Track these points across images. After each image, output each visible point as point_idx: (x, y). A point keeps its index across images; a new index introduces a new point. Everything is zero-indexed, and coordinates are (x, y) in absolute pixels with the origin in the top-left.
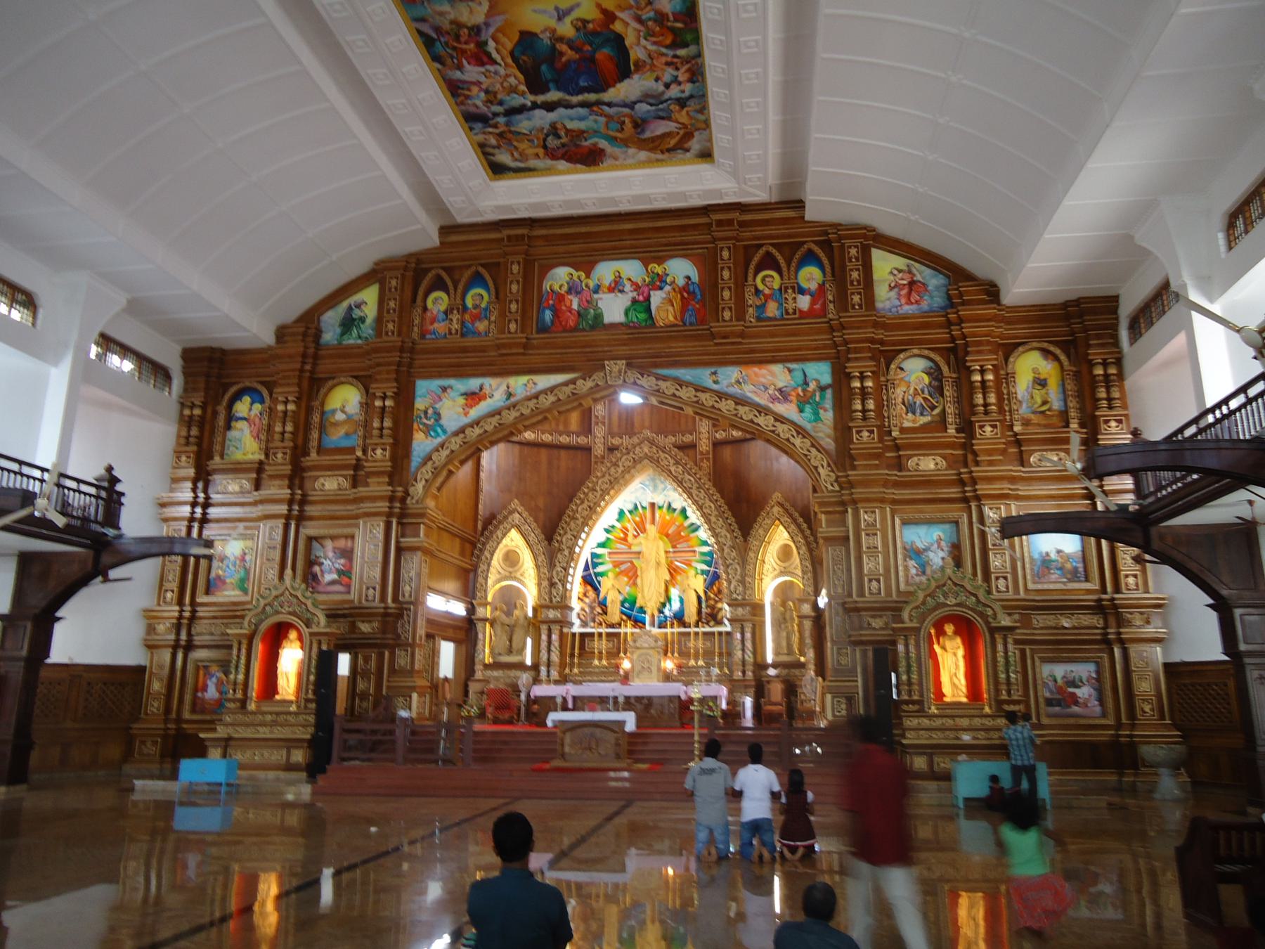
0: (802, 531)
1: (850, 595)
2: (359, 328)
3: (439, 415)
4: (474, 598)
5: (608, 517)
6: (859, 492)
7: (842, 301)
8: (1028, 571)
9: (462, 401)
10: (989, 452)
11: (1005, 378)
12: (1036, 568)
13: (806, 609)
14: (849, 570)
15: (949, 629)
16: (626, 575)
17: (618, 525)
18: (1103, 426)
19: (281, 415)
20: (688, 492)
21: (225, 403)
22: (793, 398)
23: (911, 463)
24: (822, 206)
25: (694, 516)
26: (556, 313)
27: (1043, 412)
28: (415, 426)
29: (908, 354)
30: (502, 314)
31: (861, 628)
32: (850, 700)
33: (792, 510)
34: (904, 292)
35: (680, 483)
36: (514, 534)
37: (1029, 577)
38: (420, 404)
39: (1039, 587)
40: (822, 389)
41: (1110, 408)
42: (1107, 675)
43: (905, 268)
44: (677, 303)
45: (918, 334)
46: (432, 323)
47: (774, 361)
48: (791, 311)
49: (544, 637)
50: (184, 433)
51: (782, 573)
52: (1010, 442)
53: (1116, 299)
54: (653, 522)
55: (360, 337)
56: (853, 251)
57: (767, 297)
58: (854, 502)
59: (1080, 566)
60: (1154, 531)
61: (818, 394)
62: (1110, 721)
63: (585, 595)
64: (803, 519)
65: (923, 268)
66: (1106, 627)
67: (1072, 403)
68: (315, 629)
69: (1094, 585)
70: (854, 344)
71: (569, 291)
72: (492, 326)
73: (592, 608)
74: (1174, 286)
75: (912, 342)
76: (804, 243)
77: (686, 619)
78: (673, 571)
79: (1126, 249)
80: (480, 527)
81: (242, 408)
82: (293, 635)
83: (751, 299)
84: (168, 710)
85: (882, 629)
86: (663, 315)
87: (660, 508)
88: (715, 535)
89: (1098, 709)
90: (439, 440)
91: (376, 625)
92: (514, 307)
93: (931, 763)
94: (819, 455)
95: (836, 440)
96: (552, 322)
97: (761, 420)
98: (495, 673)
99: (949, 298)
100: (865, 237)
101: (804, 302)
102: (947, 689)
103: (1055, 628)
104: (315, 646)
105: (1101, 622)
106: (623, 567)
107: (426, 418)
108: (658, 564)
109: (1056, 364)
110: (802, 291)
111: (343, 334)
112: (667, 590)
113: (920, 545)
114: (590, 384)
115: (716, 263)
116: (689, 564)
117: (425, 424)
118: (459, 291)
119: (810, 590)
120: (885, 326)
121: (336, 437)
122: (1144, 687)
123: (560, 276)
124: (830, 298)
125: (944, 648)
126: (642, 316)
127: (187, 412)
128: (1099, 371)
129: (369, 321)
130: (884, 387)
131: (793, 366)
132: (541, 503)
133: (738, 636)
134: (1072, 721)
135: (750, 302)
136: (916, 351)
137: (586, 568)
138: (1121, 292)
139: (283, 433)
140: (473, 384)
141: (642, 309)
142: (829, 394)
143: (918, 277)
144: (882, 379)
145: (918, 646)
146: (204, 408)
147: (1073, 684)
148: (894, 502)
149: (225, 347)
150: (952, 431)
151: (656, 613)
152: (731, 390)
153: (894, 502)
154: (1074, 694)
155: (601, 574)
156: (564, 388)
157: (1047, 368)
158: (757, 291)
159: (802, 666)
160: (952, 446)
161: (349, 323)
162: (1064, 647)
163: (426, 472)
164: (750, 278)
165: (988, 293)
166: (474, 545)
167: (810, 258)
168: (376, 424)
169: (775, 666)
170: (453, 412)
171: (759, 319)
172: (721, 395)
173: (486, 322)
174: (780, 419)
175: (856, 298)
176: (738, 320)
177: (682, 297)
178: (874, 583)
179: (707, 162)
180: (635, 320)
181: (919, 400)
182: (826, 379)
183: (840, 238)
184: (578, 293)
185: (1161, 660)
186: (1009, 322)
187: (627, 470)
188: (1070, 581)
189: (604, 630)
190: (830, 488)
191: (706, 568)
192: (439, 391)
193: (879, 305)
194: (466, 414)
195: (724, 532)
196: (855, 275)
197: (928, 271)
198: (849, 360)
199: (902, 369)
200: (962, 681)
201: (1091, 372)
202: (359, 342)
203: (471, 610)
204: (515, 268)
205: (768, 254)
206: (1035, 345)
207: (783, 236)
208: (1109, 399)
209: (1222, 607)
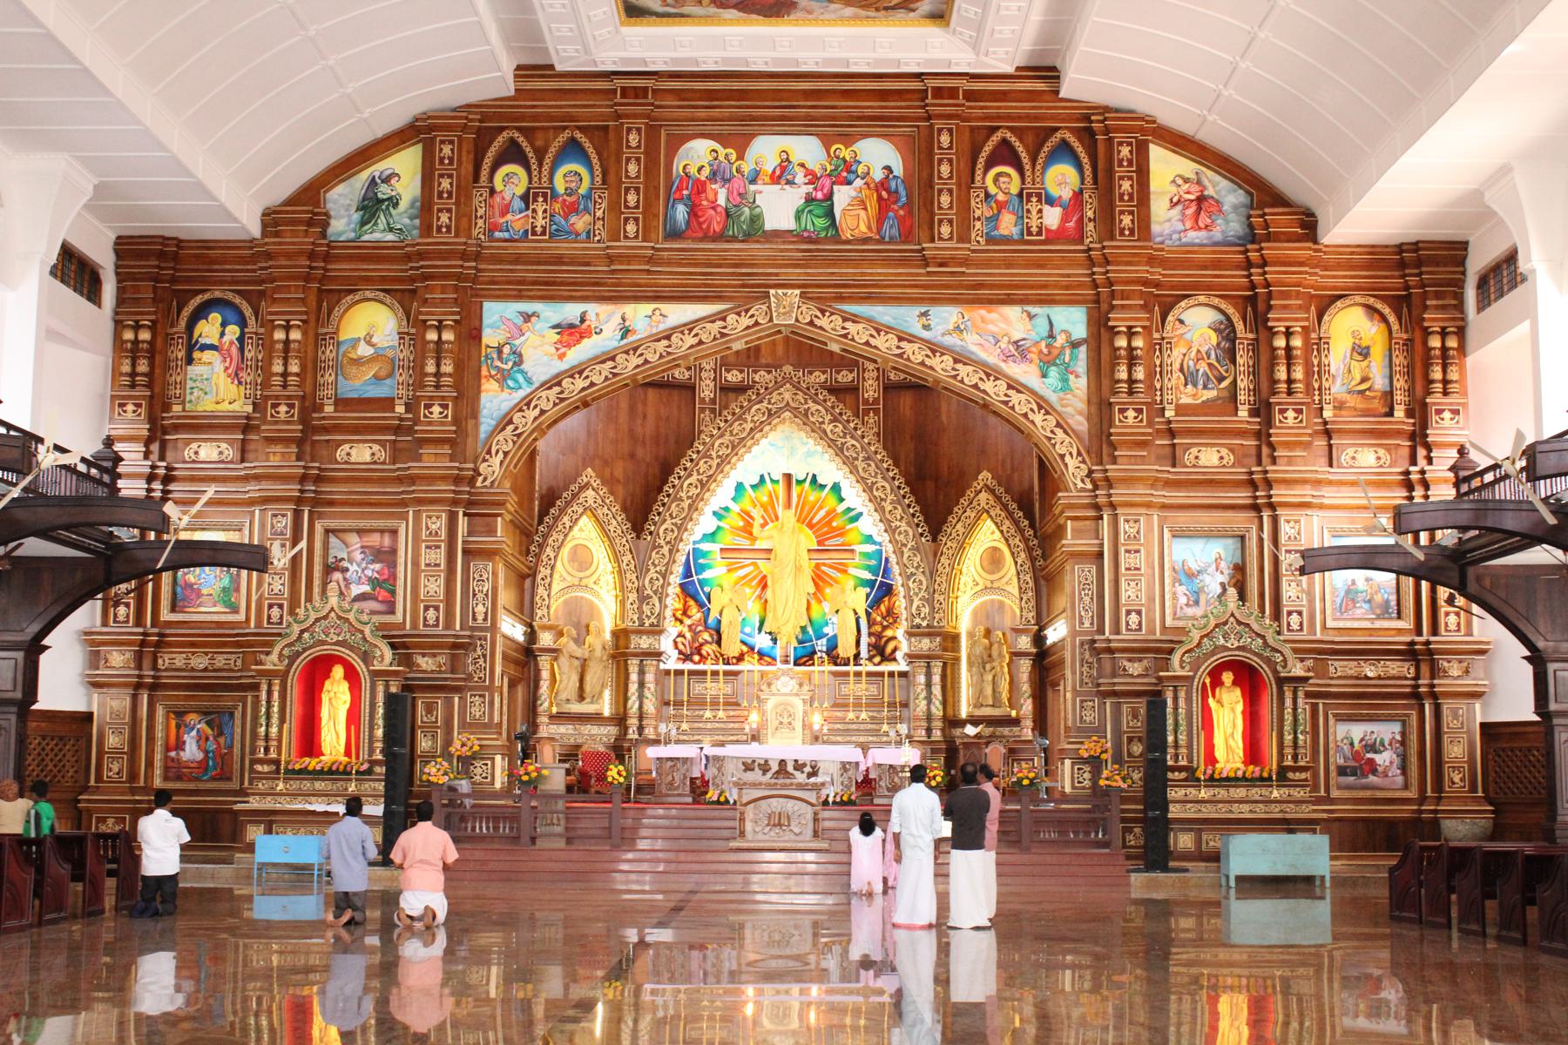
0: (1021, 531)
1: (1101, 631)
2: (388, 214)
3: (520, 355)
4: (532, 615)
5: (721, 495)
6: (1119, 494)
8: (1328, 604)
9: (553, 336)
10: (1288, 445)
11: (1318, 345)
12: (1338, 601)
13: (1025, 643)
14: (1101, 597)
15: (1228, 677)
17: (732, 505)
18: (1435, 417)
19: (280, 346)
20: (850, 463)
21: (183, 323)
22: (1034, 356)
23: (1188, 458)
24: (1082, 82)
25: (854, 497)
26: (694, 212)
27: (1362, 392)
28: (484, 372)
29: (1192, 301)
30: (615, 207)
31: (1114, 675)
33: (1006, 498)
34: (1190, 211)
35: (840, 451)
36: (586, 523)
37: (1328, 612)
38: (490, 337)
39: (1341, 624)
40: (1075, 345)
41: (1445, 393)
42: (1414, 737)
43: (1193, 176)
46: (503, 214)
47: (1009, 301)
48: (1034, 230)
49: (634, 677)
50: (126, 368)
52: (1316, 432)
53: (1463, 246)
54: (788, 505)
55: (391, 230)
56: (1125, 151)
57: (1001, 206)
58: (1112, 506)
59: (1393, 598)
60: (1471, 572)
61: (1068, 352)
62: (1413, 794)
63: (685, 613)
65: (1218, 178)
66: (1417, 678)
67: (1400, 383)
68: (377, 667)
69: (1407, 624)
70: (1118, 286)
71: (713, 176)
72: (599, 224)
73: (696, 634)
74: (1523, 266)
75: (1197, 287)
76: (1057, 129)
78: (820, 580)
79: (1476, 206)
81: (208, 330)
82: (338, 671)
83: (980, 209)
84: (133, 776)
85: (1139, 676)
86: (851, 222)
87: (799, 482)
88: (891, 530)
89: (1400, 779)
91: (442, 659)
92: (632, 198)
93: (1199, 842)
94: (1068, 439)
95: (1088, 420)
96: (688, 223)
97: (988, 386)
98: (562, 729)
99: (1251, 226)
100: (1142, 130)
101: (1052, 217)
102: (1220, 753)
103: (1357, 678)
104: (380, 689)
105: (1412, 670)
106: (742, 573)
108: (798, 569)
109: (1383, 326)
110: (1051, 202)
111: (363, 223)
113: (1194, 567)
114: (746, 321)
115: (931, 154)
116: (845, 572)
117: (499, 369)
120: (1164, 263)
121: (359, 384)
122: (1455, 751)
123: (698, 154)
124: (1090, 214)
125: (1220, 702)
126: (821, 223)
127: (128, 335)
129: (403, 204)
130: (1158, 346)
131: (1033, 309)
132: (619, 472)
133: (922, 679)
134: (1368, 794)
135: (978, 213)
136: (1202, 299)
137: (687, 573)
138: (1471, 239)
139: (285, 374)
140: (570, 311)
141: (819, 211)
142: (1083, 351)
143: (1210, 192)
144: (1156, 335)
145: (1189, 700)
146: (153, 328)
147: (1373, 748)
148: (1164, 507)
149: (183, 236)
150: (1243, 413)
151: (794, 643)
152: (949, 341)
153: (1164, 507)
154: (1371, 761)
156: (709, 325)
157: (1372, 332)
158: (987, 195)
159: (1016, 722)
161: (371, 206)
162: (1365, 702)
163: (505, 441)
164: (978, 178)
165: (1303, 225)
167: (1064, 151)
168: (430, 368)
169: (975, 721)
170: (541, 355)
171: (990, 240)
172: (935, 349)
173: (587, 218)
174: (1014, 385)
175: (1127, 220)
176: (960, 240)
177: (880, 198)
179: (939, 26)
180: (810, 227)
181: (1203, 367)
182: (1080, 331)
183: (1107, 130)
184: (726, 181)
185: (1479, 720)
187: (757, 428)
188: (1378, 618)
189: (721, 667)
190: (1080, 485)
191: (869, 576)
192: (519, 321)
193: (1155, 228)
194: (561, 357)
195: (904, 526)
196: (1126, 185)
197: (1224, 184)
198: (1112, 307)
199: (1181, 322)
200: (1238, 744)
201: (1425, 343)
202: (390, 237)
203: (532, 635)
204: (633, 139)
206: (1358, 299)
207: (1028, 118)
208: (1445, 382)
209: (1537, 660)
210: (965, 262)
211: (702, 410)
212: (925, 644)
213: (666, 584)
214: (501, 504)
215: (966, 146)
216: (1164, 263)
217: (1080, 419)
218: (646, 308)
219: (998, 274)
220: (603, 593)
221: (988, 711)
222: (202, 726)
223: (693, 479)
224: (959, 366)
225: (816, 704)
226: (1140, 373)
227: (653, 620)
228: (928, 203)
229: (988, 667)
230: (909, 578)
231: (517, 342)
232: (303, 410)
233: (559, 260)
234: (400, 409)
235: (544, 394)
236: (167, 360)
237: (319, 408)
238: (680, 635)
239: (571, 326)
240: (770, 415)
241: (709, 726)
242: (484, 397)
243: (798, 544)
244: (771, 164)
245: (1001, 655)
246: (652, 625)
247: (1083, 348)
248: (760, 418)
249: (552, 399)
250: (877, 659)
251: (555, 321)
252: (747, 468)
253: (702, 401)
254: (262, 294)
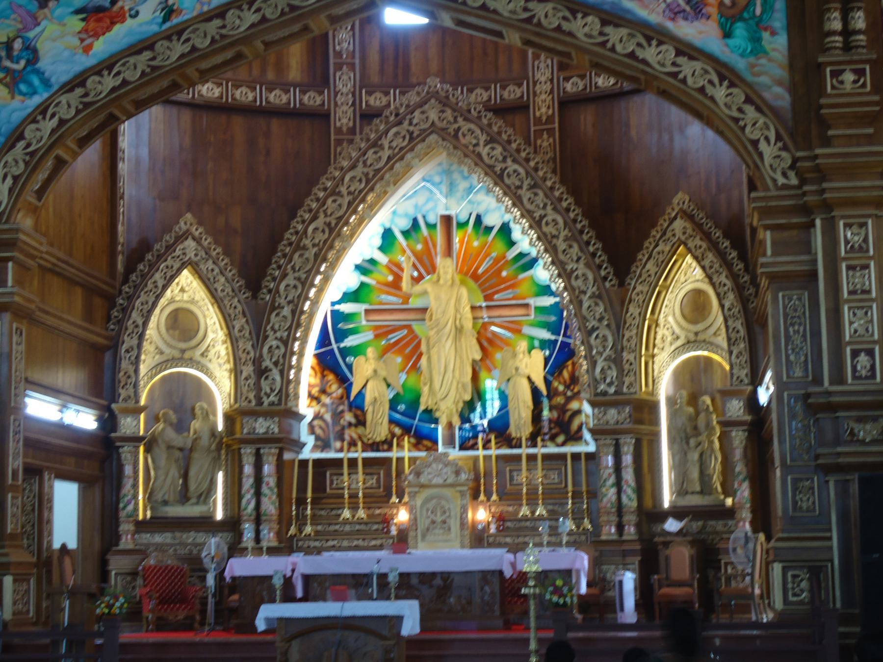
3: (35, 51)
4: (114, 398)
5: (365, 244)
6: (836, 188)
9: (76, 24)
13: (736, 408)
16: (400, 352)
22: (713, 10)
31: (837, 442)
32: (816, 573)
33: (708, 225)
35: (499, 178)
36: (186, 277)
49: (248, 469)
51: (690, 344)
58: (827, 207)
63: (323, 391)
64: (730, 243)
73: (337, 416)
77: (513, 431)
78: (488, 344)
80: (120, 266)
87: (462, 225)
88: (564, 273)
90: (37, 100)
94: (762, 121)
95: (793, 89)
97: (650, 54)
98: (158, 538)
106: (395, 337)
107: (10, 57)
108: (459, 330)
112: (475, 378)
116: (517, 331)
117: (8, 71)
119: (744, 373)
132: (236, 218)
133: (610, 460)
137: (324, 339)
151: (456, 422)
155: (355, 351)
159: (730, 513)
166: (110, 301)
174: (686, 50)
178: (863, 358)
187: (398, 156)
190: (781, 180)
191: (546, 335)
194: (87, 49)
195: (581, 268)
203: (108, 421)
211: (339, 142)
212: (612, 414)
217: (778, 90)
220: (213, 366)
223: (320, 222)
224: (609, 29)
225: (482, 497)
227: (272, 398)
229: (692, 442)
230: (590, 333)
231: (31, 34)
235: (63, 99)
238: (317, 416)
239: (100, 9)
240: (411, 139)
241: (347, 528)
243: (458, 300)
245: (709, 426)
246: (272, 404)
248: (399, 142)
249: (74, 103)
250: (561, 439)
253: (339, 131)
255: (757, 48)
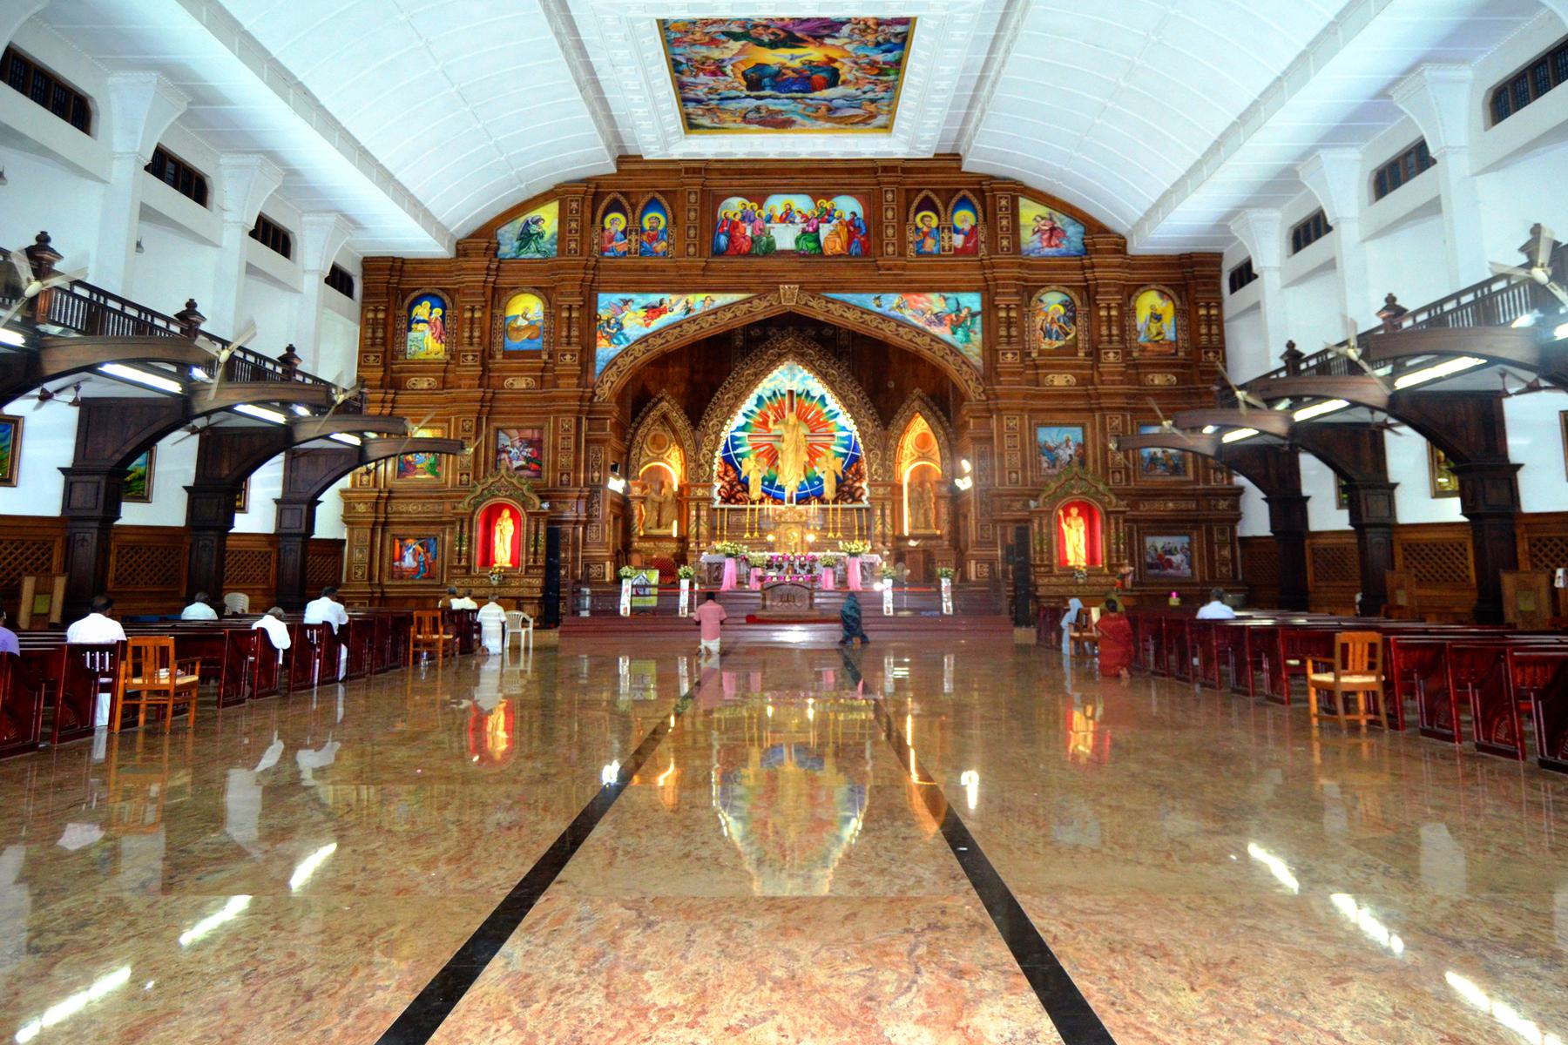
2: (536, 242)
6: (1003, 403)
7: (993, 238)
9: (642, 313)
11: (1127, 312)
15: (1074, 511)
26: (731, 239)
32: (991, 564)
38: (603, 313)
40: (973, 315)
44: (844, 236)
45: (1058, 275)
47: (931, 290)
56: (1003, 202)
57: (926, 234)
58: (999, 410)
71: (743, 219)
81: (422, 311)
83: (911, 237)
84: (371, 578)
86: (831, 245)
90: (622, 347)
100: (1014, 190)
101: (958, 240)
110: (957, 231)
111: (521, 248)
118: (638, 212)
120: (1029, 267)
121: (517, 342)
123: (734, 206)
126: (812, 245)
128: (1202, 312)
129: (547, 236)
140: (654, 298)
142: (979, 318)
143: (1058, 224)
146: (386, 311)
147: (1170, 552)
150: (1081, 354)
152: (893, 313)
153: (1032, 410)
160: (1080, 367)
161: (526, 237)
167: (964, 203)
170: (635, 324)
171: (919, 254)
172: (885, 318)
174: (935, 339)
181: (1055, 327)
182: (977, 307)
183: (992, 190)
184: (751, 222)
186: (1129, 266)
193: (1024, 247)
197: (1067, 220)
198: (997, 294)
200: (1082, 552)
205: (927, 198)
210: (904, 268)
213: (713, 457)
214: (610, 412)
215: (902, 200)
216: (1029, 267)
218: (702, 296)
219: (925, 275)
221: (922, 531)
222: (417, 546)
226: (1014, 332)
228: (879, 234)
232: (483, 357)
233: (646, 269)
234: (545, 357)
236: (395, 329)
237: (492, 356)
242: (598, 350)
244: (779, 211)
247: (979, 318)
251: (644, 303)
252: (765, 387)
254: (457, 290)
255: (968, 340)
